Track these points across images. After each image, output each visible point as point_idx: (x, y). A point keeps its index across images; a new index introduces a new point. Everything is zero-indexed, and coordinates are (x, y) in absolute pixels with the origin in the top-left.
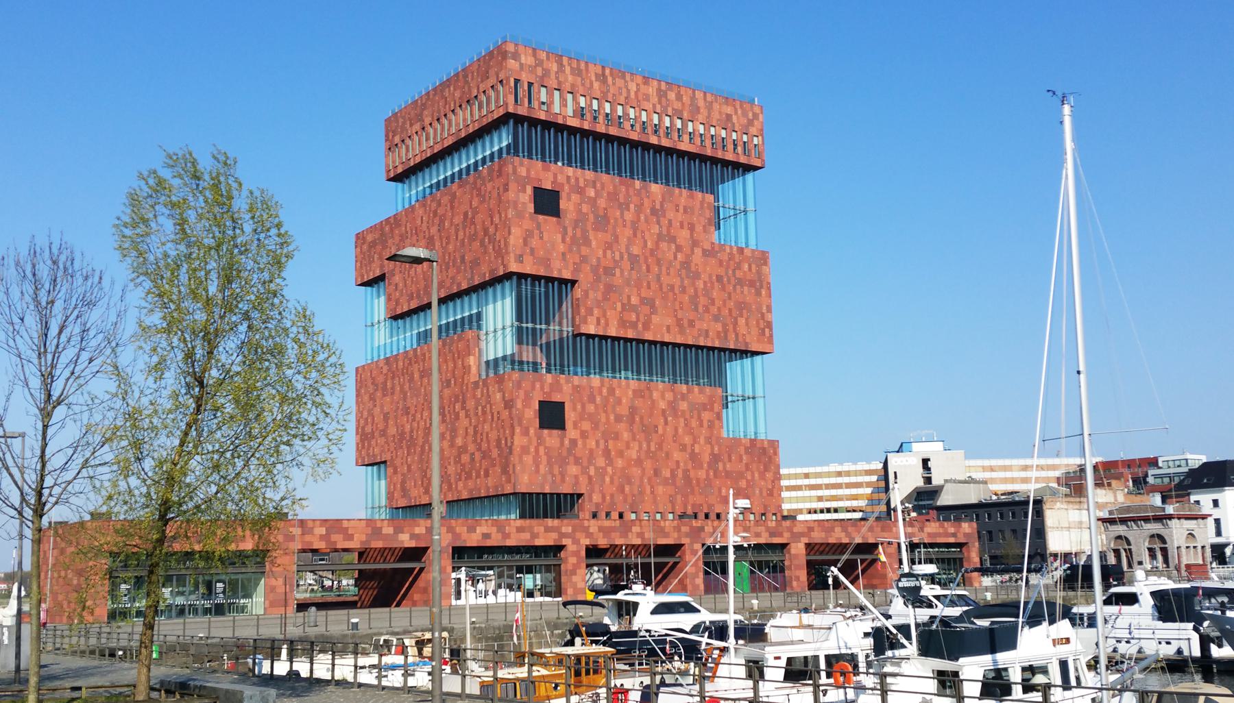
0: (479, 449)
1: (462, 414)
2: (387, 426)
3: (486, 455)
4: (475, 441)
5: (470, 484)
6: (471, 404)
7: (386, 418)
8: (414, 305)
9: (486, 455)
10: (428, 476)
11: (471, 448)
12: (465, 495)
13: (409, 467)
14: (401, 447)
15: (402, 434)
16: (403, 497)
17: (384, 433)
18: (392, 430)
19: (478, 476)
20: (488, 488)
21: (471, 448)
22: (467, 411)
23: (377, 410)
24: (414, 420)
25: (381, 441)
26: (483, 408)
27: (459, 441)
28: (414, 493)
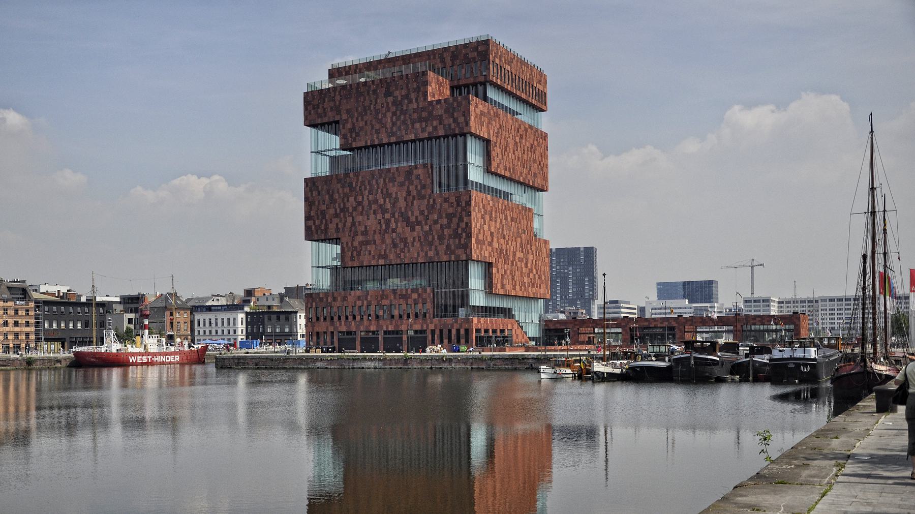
0: (537, 273)
1: (530, 251)
2: (492, 240)
3: (540, 277)
4: (536, 268)
5: (534, 289)
6: (534, 248)
7: (492, 234)
8: (507, 174)
9: (540, 277)
10: (515, 280)
11: (534, 271)
12: (531, 296)
13: (505, 271)
14: (501, 258)
15: (501, 250)
16: (502, 288)
17: (490, 244)
18: (496, 245)
19: (537, 287)
20: (540, 294)
21: (534, 271)
22: (532, 251)
23: (486, 227)
24: (508, 244)
25: (490, 248)
26: (539, 253)
27: (529, 265)
28: (508, 287)
